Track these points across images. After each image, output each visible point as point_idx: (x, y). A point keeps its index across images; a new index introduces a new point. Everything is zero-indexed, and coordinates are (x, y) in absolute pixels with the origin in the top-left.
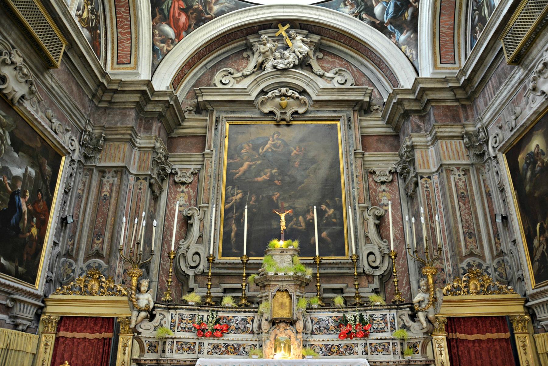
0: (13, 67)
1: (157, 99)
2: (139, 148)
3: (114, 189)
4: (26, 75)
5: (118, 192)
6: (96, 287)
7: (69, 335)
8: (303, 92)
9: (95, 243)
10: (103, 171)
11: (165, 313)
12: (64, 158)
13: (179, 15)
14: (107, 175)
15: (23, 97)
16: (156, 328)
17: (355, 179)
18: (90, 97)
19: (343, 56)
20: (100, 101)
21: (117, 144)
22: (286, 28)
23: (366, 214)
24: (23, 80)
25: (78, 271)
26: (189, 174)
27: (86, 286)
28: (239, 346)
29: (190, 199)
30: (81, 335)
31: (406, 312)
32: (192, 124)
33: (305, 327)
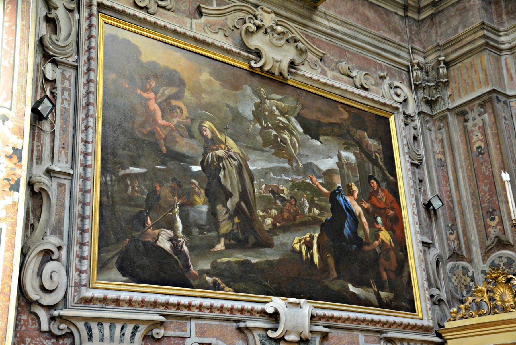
0: (262, 31)
2: (510, 49)
3: (489, 132)
4: (283, 33)
5: (497, 135)
9: (490, 226)
10: (461, 112)
12: (392, 119)
14: (470, 116)
15: (292, 64)
18: (401, 13)
20: (419, 11)
21: (467, 61)
24: (283, 42)
25: (480, 278)
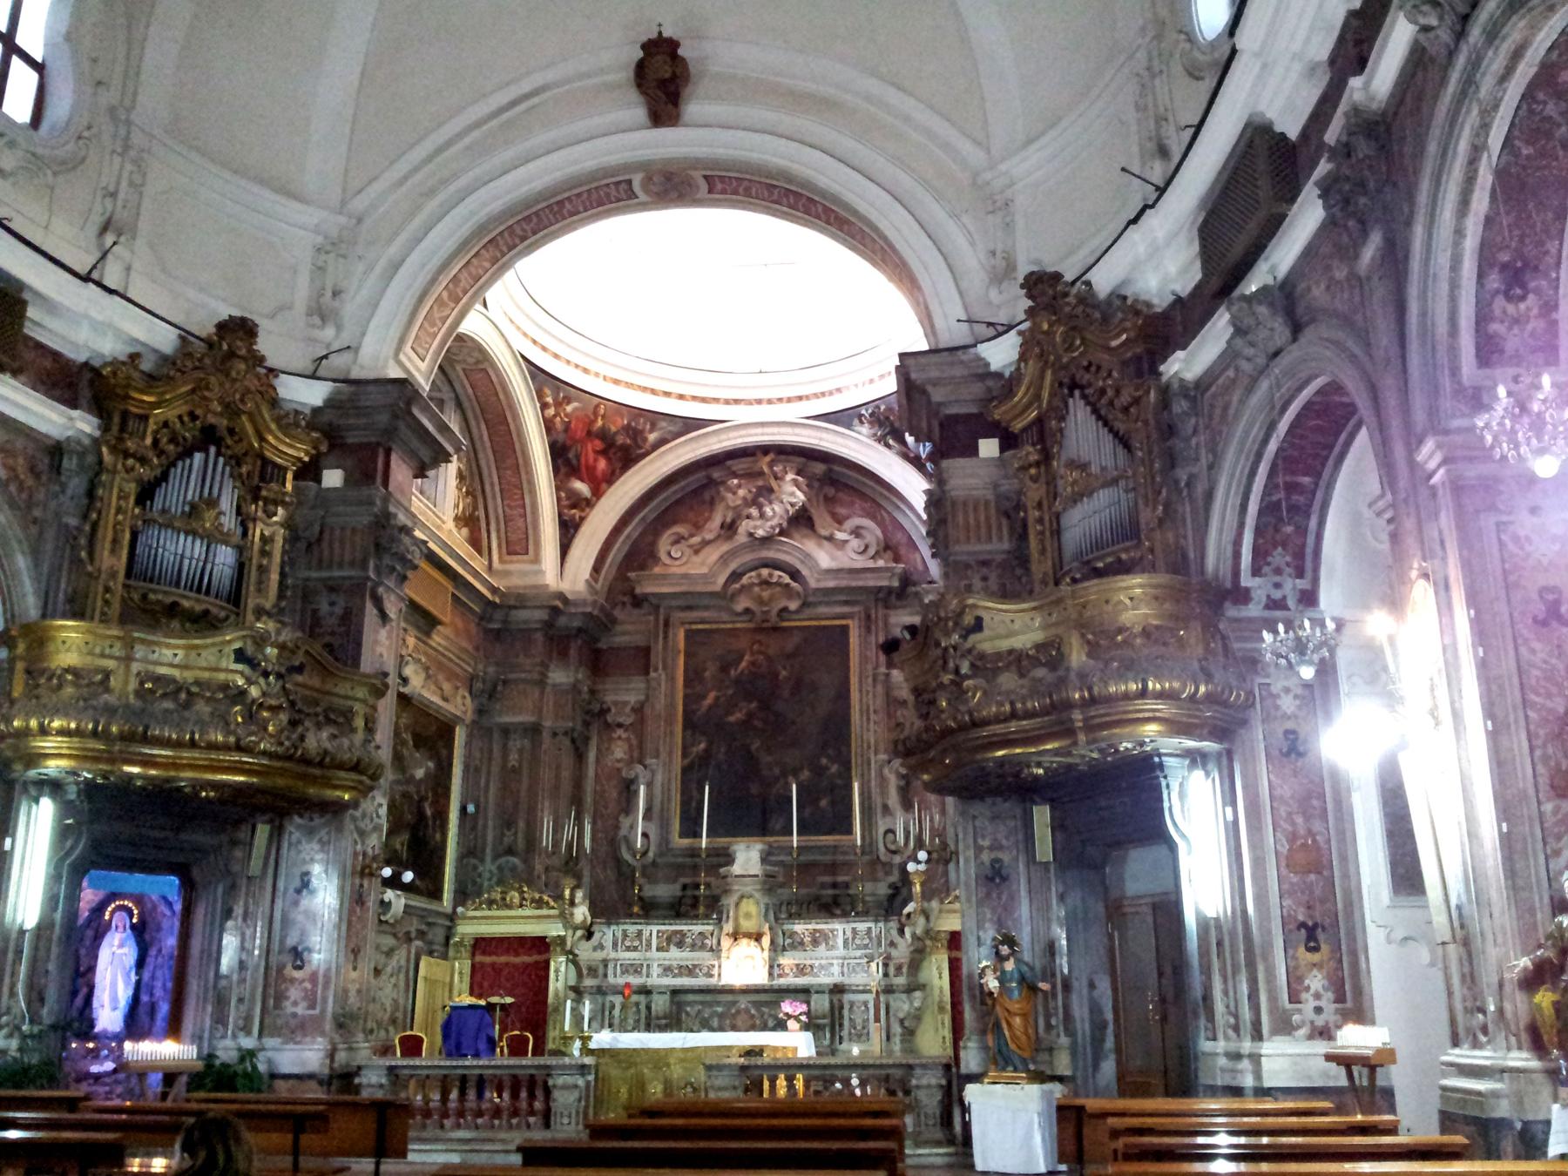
1: (573, 610)
2: (554, 685)
6: (517, 901)
7: (488, 959)
8: (795, 575)
10: (506, 731)
13: (596, 460)
16: (595, 949)
17: (872, 716)
19: (868, 492)
20: (490, 620)
21: (521, 687)
22: (768, 459)
23: (886, 771)
25: (487, 875)
26: (628, 710)
27: (504, 899)
30: (503, 959)
31: (894, 925)
32: (629, 630)
33: (772, 942)
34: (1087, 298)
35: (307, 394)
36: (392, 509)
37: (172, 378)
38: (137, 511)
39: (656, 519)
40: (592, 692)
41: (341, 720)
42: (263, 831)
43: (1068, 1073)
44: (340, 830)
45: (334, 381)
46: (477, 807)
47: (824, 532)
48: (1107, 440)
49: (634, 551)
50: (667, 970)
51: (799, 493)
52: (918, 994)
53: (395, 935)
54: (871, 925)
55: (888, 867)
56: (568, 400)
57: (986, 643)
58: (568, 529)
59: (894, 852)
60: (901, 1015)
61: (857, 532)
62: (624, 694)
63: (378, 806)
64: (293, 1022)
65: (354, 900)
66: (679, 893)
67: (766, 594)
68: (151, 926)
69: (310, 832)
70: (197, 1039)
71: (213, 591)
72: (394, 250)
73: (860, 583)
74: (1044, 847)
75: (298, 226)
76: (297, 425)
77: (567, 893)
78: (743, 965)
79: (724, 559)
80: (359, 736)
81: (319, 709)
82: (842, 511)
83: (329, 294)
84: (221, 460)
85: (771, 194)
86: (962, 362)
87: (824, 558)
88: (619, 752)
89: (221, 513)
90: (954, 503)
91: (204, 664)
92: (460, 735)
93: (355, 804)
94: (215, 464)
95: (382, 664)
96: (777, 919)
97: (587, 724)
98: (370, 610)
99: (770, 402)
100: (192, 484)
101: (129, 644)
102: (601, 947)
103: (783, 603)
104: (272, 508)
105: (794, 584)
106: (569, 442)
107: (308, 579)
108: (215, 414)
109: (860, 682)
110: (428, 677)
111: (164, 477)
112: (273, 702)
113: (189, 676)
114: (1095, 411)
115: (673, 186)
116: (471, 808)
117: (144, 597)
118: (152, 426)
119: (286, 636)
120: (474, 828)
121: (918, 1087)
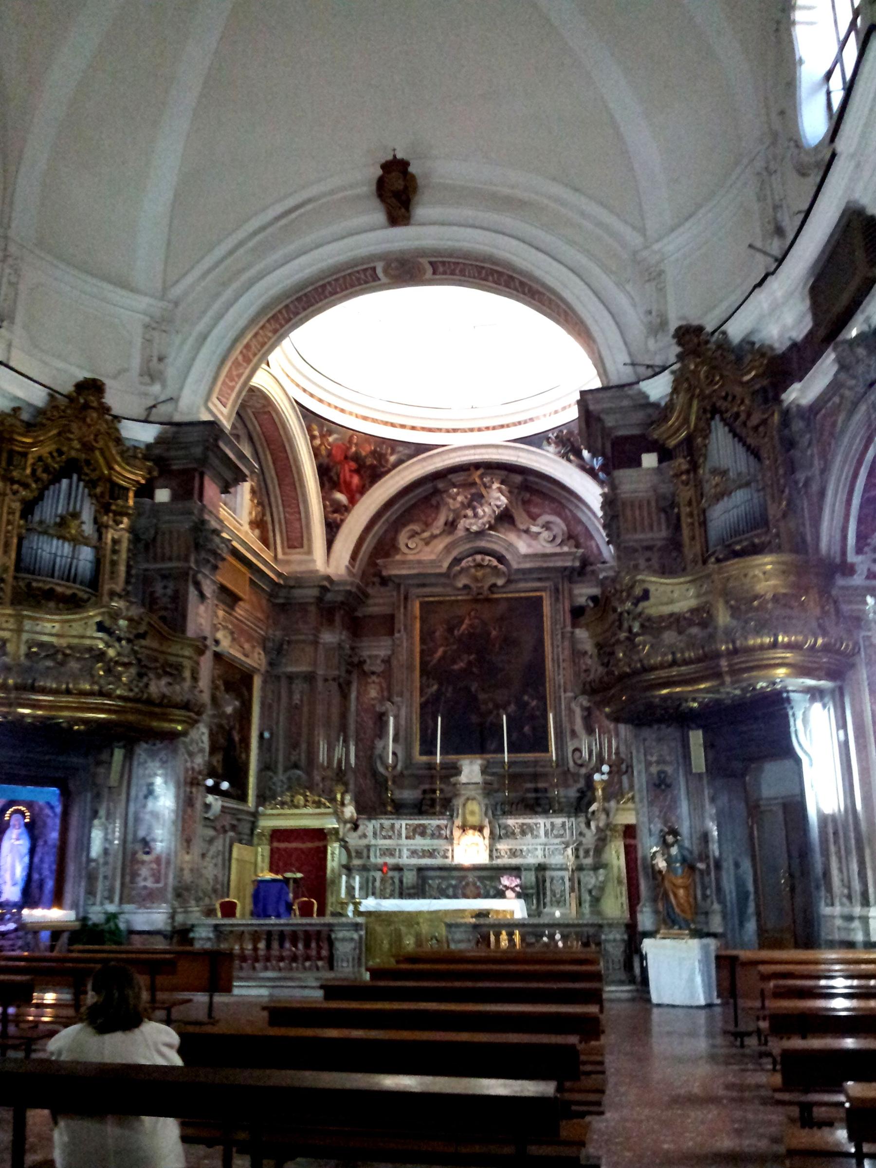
6: (302, 802)
7: (283, 845)
8: (501, 559)
10: (291, 678)
11: (366, 822)
13: (351, 477)
16: (360, 838)
20: (277, 597)
22: (479, 472)
23: (573, 705)
26: (379, 661)
27: (292, 801)
28: (434, 850)
29: (382, 690)
31: (582, 819)
32: (378, 603)
33: (492, 833)
34: (724, 345)
35: (142, 434)
36: (207, 517)
37: (43, 425)
38: (22, 522)
39: (397, 518)
40: (353, 648)
41: (174, 672)
42: (118, 754)
43: (720, 930)
44: (175, 751)
45: (161, 423)
46: (272, 734)
47: (522, 527)
48: (740, 449)
49: (380, 545)
50: (414, 853)
51: (503, 498)
52: (601, 871)
53: (215, 828)
54: (566, 820)
55: (576, 776)
56: (330, 433)
57: (653, 608)
58: (332, 529)
59: (581, 766)
60: (590, 887)
61: (547, 526)
62: (376, 650)
63: (201, 735)
64: (144, 892)
65: (186, 803)
66: (421, 797)
67: (480, 574)
68: (39, 823)
69: (152, 755)
70: (75, 906)
71: (79, 578)
72: (201, 327)
73: (551, 565)
74: (699, 759)
75: (132, 309)
76: (135, 457)
77: (339, 796)
78: (470, 849)
79: (448, 549)
80: (187, 684)
81: (158, 665)
82: (535, 510)
83: (155, 359)
84: (82, 484)
85: (480, 273)
86: (628, 396)
87: (523, 546)
88: (373, 693)
89: (83, 523)
90: (624, 504)
91: (74, 633)
92: (257, 682)
93: (184, 733)
94: (78, 486)
95: (202, 630)
96: (494, 815)
97: (349, 672)
98: (192, 592)
99: (480, 430)
100: (61, 501)
101: (20, 619)
102: (364, 836)
103: (493, 580)
104: (118, 518)
105: (500, 566)
106: (331, 464)
107: (146, 570)
108: (77, 450)
109: (552, 639)
110: (234, 639)
111: (40, 498)
112: (126, 660)
113: (63, 642)
114: (732, 431)
115: (406, 270)
116: (267, 735)
117: (29, 585)
118: (30, 461)
119: (135, 611)
120: (269, 750)
121: (606, 941)
